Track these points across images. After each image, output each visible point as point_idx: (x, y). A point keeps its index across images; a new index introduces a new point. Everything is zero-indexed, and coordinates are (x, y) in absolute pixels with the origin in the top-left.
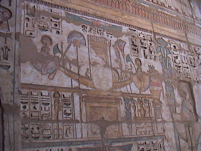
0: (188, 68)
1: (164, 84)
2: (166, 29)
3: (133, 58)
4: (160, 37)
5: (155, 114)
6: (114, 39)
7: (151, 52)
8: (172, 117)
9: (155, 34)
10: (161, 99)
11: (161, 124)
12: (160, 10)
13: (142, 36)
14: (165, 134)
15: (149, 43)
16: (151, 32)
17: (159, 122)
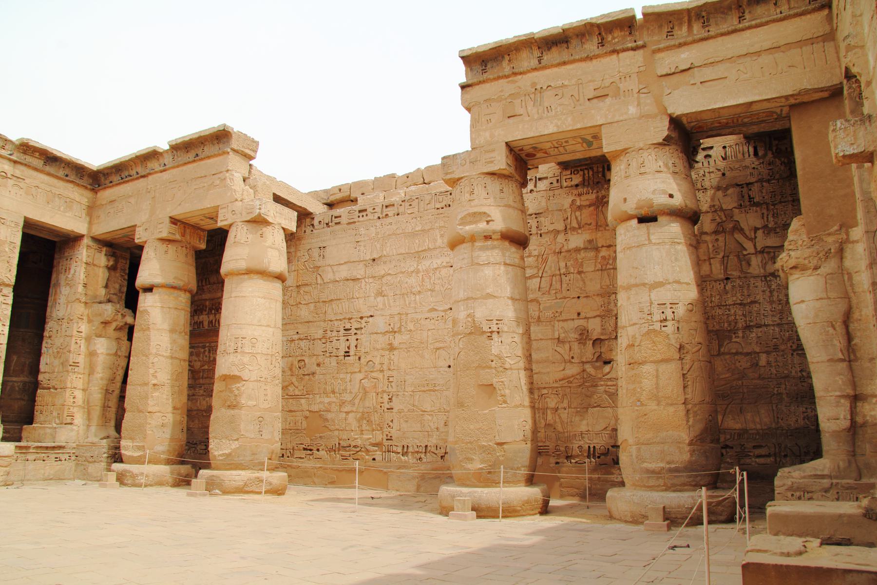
3: (208, 356)
6: (203, 350)
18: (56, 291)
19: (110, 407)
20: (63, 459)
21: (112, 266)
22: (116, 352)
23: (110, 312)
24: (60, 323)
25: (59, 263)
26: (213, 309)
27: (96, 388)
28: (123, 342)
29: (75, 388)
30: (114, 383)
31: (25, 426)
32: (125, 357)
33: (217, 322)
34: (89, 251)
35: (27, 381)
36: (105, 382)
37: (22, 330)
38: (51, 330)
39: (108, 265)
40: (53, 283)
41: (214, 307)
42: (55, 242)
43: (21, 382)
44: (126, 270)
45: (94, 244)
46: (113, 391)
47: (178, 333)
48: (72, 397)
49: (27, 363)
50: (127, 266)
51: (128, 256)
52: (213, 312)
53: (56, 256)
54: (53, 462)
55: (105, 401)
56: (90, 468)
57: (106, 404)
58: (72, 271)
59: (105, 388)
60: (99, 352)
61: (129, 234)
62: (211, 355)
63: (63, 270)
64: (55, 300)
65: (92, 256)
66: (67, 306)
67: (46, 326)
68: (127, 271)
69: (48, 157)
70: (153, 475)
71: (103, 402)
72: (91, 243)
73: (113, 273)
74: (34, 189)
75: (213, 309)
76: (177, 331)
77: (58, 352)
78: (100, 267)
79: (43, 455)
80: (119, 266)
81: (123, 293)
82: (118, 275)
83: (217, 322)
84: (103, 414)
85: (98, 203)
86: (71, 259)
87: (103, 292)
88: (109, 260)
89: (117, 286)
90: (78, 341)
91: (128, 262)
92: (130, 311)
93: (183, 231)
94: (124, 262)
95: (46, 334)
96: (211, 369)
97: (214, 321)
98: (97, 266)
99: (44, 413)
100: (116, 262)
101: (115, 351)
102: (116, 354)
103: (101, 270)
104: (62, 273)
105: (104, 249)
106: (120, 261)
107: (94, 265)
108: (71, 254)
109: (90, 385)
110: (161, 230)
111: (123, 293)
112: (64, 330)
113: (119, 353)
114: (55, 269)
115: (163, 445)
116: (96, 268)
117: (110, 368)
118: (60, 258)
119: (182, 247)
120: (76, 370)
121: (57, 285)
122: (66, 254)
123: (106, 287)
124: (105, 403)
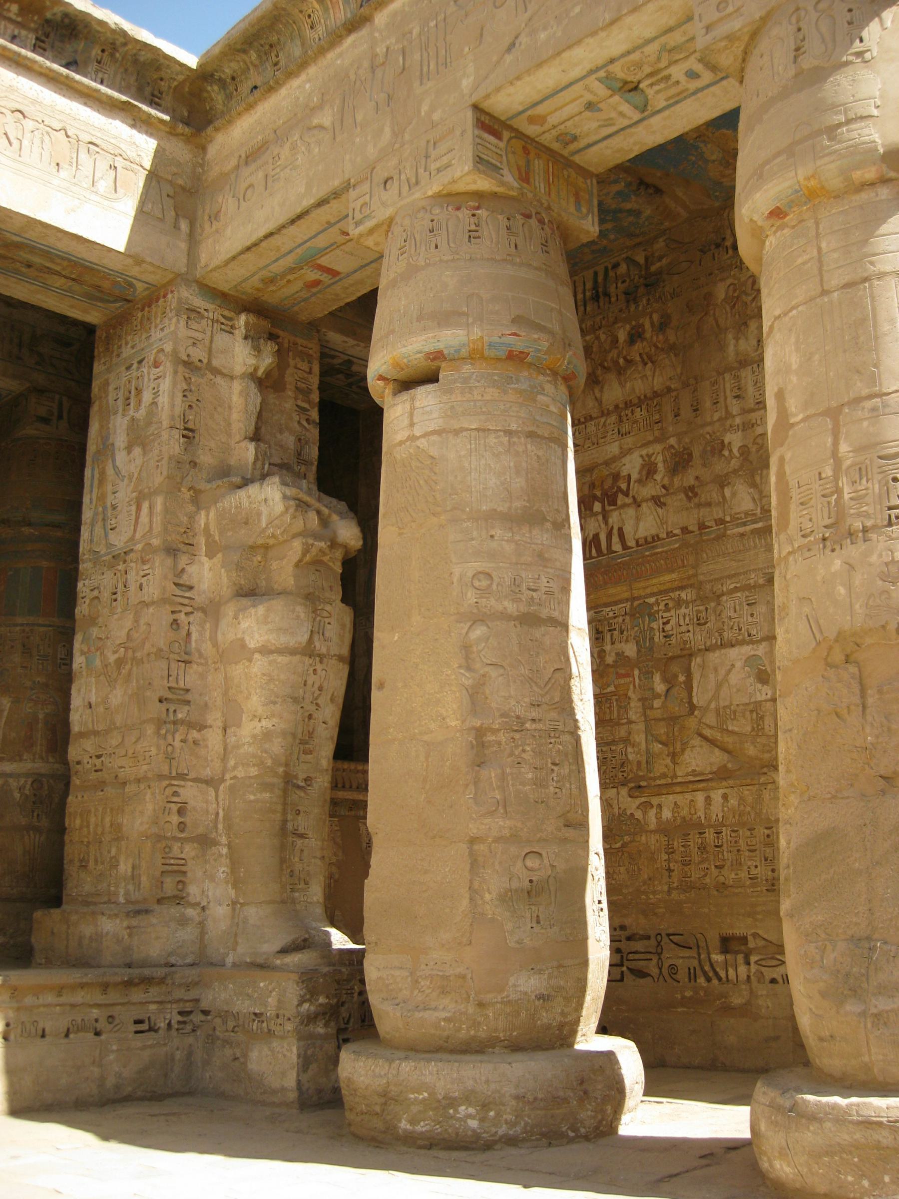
0: (689, 631)
1: (636, 672)
2: (655, 581)
4: (641, 601)
5: (619, 713)
7: (622, 633)
8: (645, 714)
9: (634, 599)
10: (630, 694)
11: (625, 727)
12: (647, 553)
13: (611, 614)
14: (631, 738)
15: (620, 619)
16: (627, 600)
17: (623, 724)
18: (103, 473)
19: (302, 836)
20: (163, 1025)
21: (268, 373)
22: (310, 641)
23: (279, 507)
24: (121, 567)
25: (107, 383)
26: (595, 498)
27: (253, 771)
28: (328, 608)
29: (182, 776)
30: (311, 752)
31: (38, 914)
32: (341, 658)
33: (615, 539)
34: (195, 326)
35: (43, 771)
36: (277, 747)
37: (20, 620)
38: (96, 593)
39: (256, 369)
40: (92, 447)
41: (598, 493)
42: (90, 329)
43: (27, 775)
44: (309, 391)
45: (211, 307)
46: (307, 780)
47: (548, 525)
48: (174, 807)
49: (41, 716)
50: (315, 381)
51: (314, 349)
52: (597, 507)
53: (98, 368)
54: (131, 1035)
55: (284, 812)
56: (254, 1055)
57: (290, 826)
58: (147, 397)
59: (281, 770)
60: (252, 644)
61: (321, 242)
62: (608, 647)
63: (120, 402)
64: (102, 498)
65: (207, 342)
66: (139, 509)
67: (80, 585)
68: (315, 397)
69: (48, 21)
70: (517, 1098)
71: (278, 817)
72: (199, 302)
73: (272, 398)
74: (10, 118)
75: (595, 498)
76: (545, 519)
77: (120, 663)
78: (232, 378)
79: (95, 1013)
80: (290, 377)
81: (306, 463)
82: (289, 405)
83: (615, 539)
84: (282, 861)
85: (214, 172)
86: (140, 362)
87: (249, 451)
88: (257, 349)
89: (290, 441)
90: (182, 617)
91: (316, 369)
92: (342, 506)
93: (522, 163)
94: (305, 366)
95: (82, 609)
96: (613, 694)
97: (603, 537)
98: (224, 375)
99: (91, 864)
100: (280, 353)
101: (306, 637)
102: (308, 651)
103: (237, 386)
104: (115, 413)
105: (243, 318)
106: (292, 362)
107: (216, 372)
108: (138, 348)
109: (232, 763)
110: (445, 160)
111: (306, 463)
112: (133, 587)
113: (320, 646)
114: (94, 409)
115: (540, 972)
116: (219, 380)
117: (295, 700)
118: (109, 370)
119: (528, 216)
120: (180, 716)
121: (107, 449)
122: (127, 352)
123: (256, 437)
124: (285, 822)
